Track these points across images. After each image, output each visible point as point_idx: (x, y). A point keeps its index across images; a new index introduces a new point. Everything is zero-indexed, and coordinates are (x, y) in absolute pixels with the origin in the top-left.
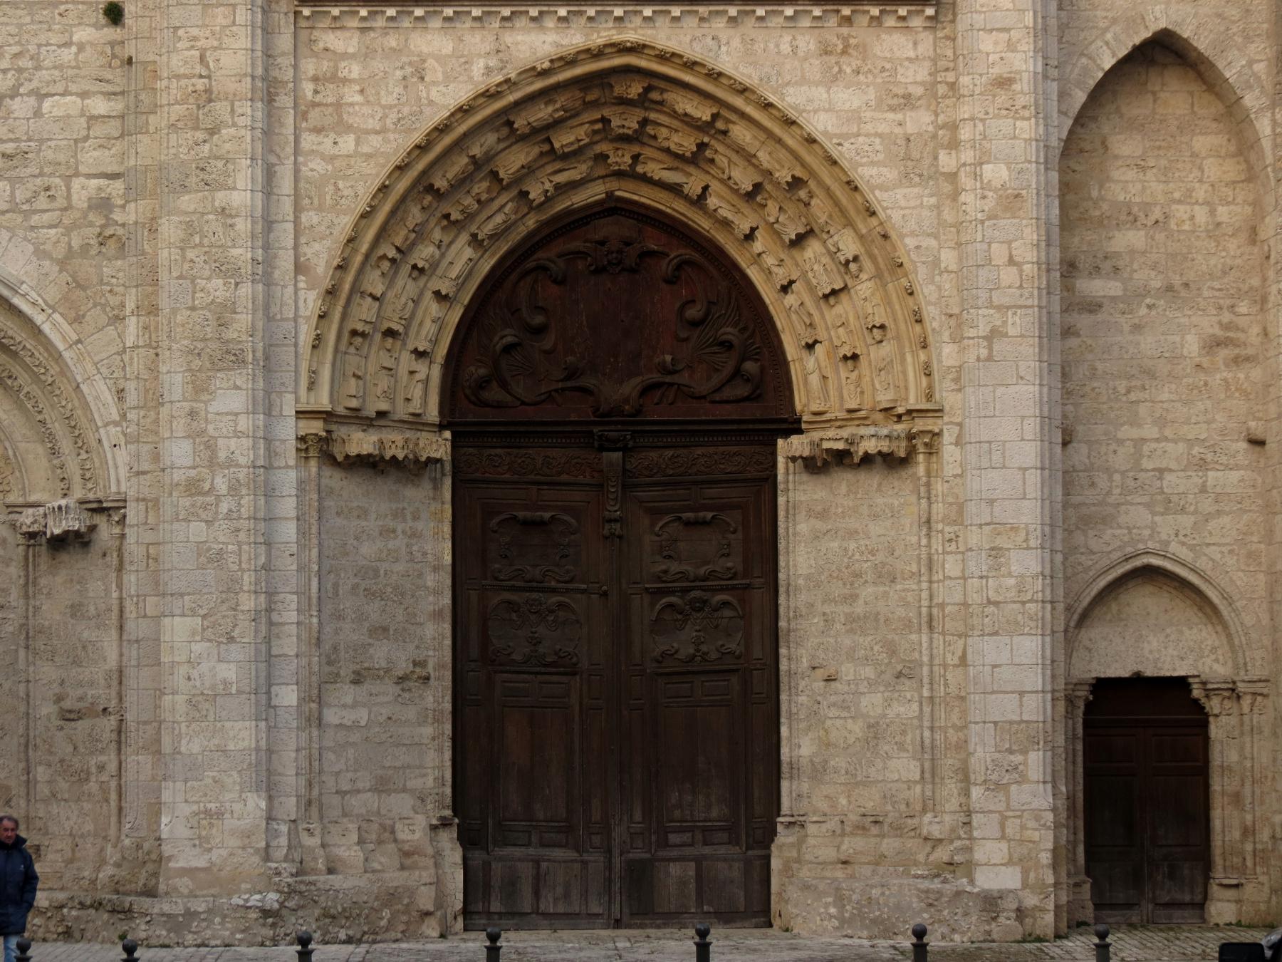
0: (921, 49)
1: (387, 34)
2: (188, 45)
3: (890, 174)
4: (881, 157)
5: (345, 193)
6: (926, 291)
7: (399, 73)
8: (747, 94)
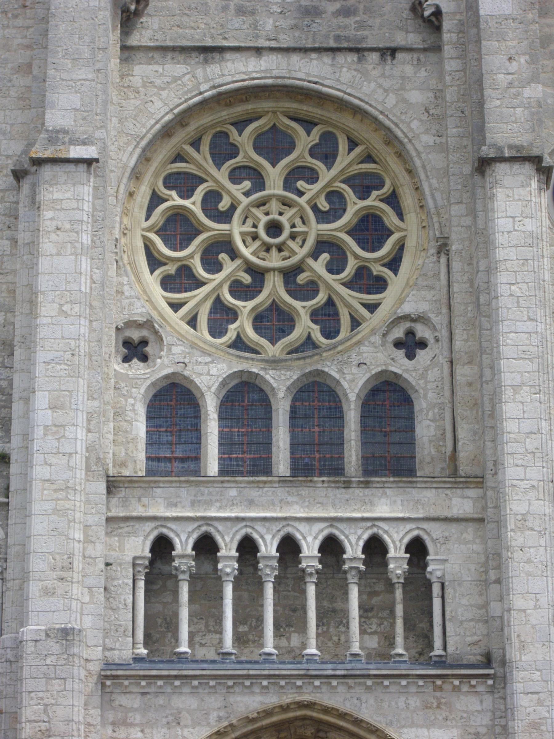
0: (485, 704)
1: (157, 696)
2: (36, 702)
7: (165, 721)
8: (378, 733)
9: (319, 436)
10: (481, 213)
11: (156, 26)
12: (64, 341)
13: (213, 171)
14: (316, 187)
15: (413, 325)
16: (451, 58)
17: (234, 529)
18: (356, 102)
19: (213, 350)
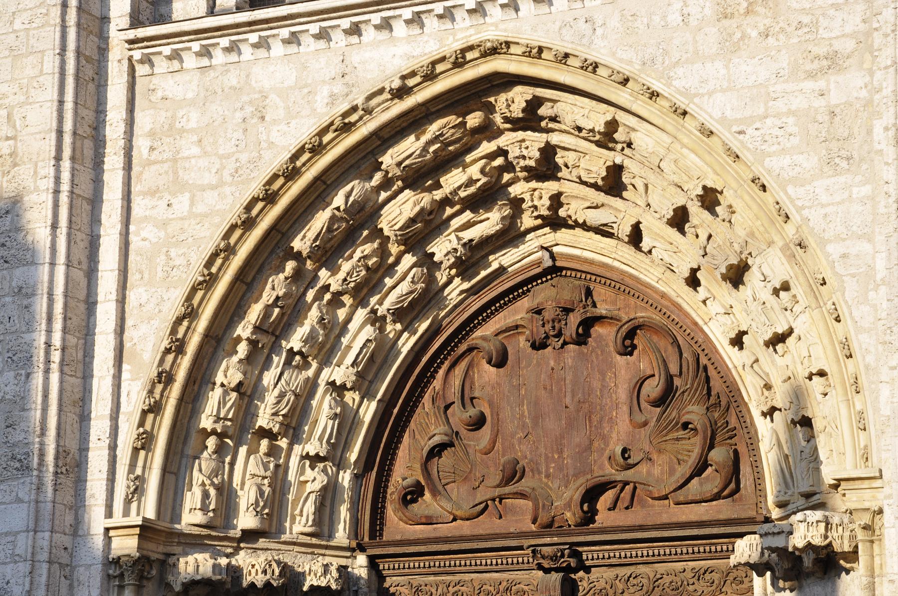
1: (228, 71)
3: (809, 162)
4: (795, 141)
5: (177, 263)
6: (855, 314)
7: (239, 115)
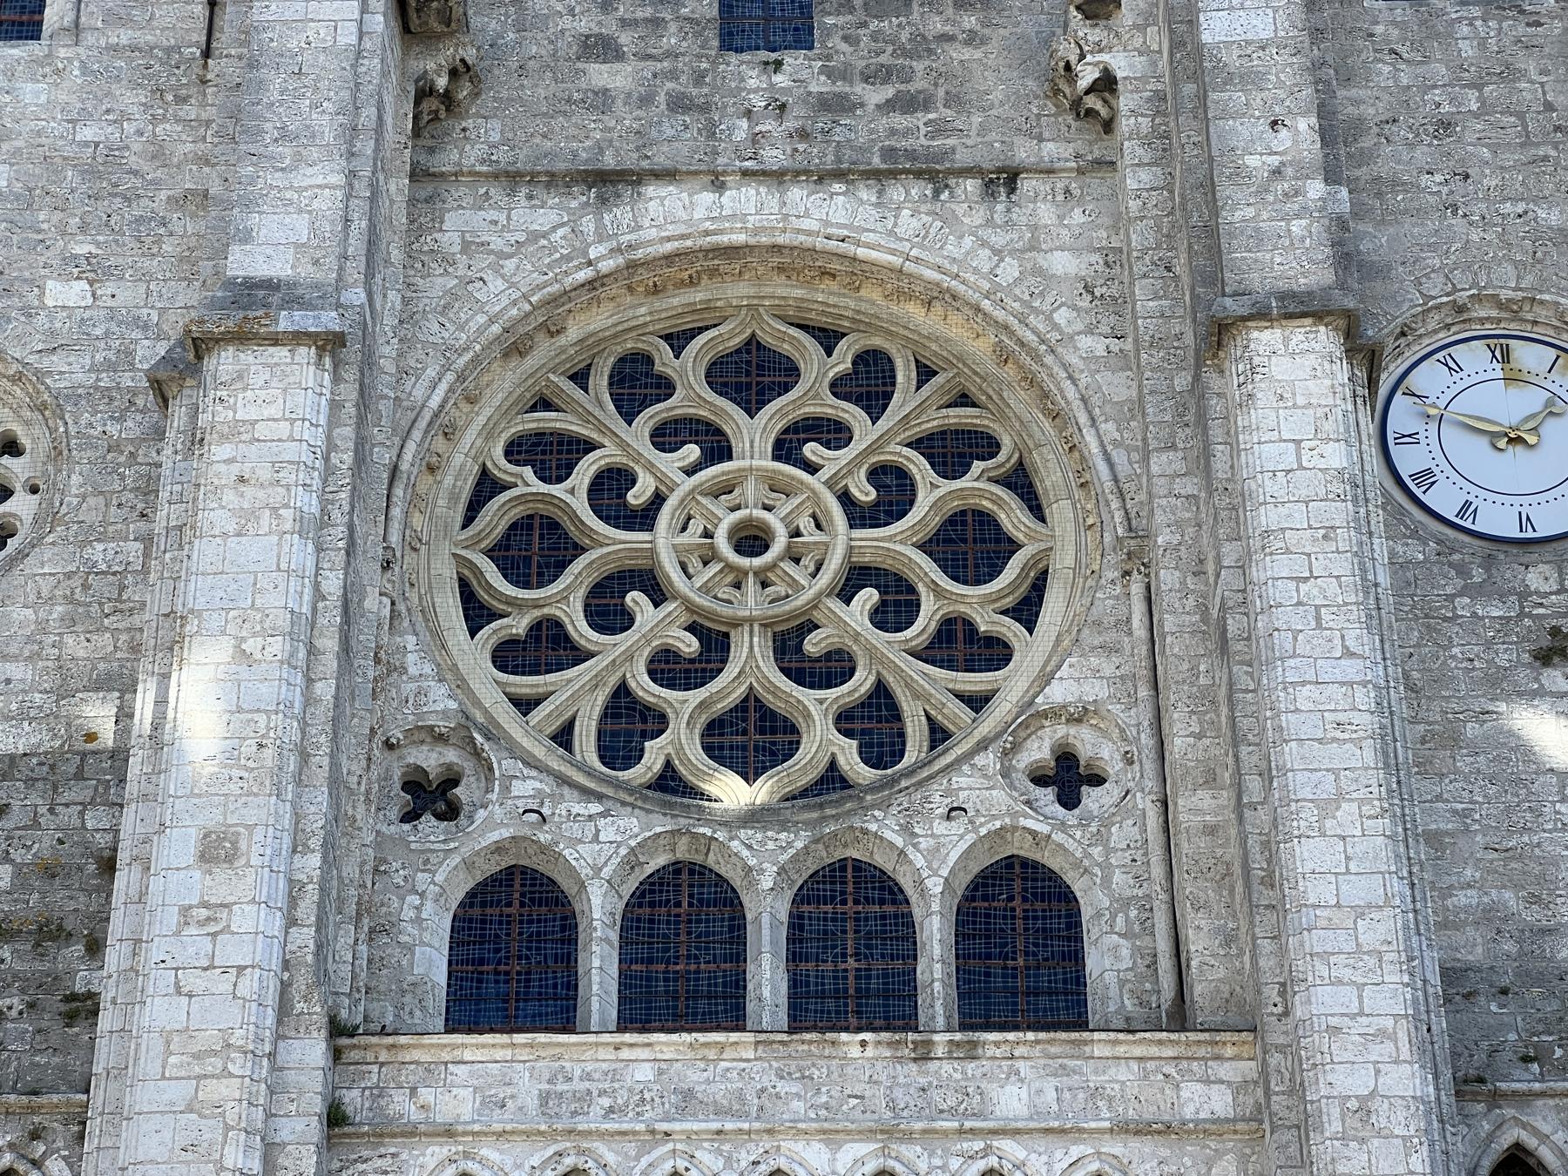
9: (857, 978)
10: (1220, 447)
11: (495, 137)
12: (241, 716)
13: (618, 425)
14: (846, 454)
15: (1072, 731)
16: (1138, 165)
17: (644, 1161)
18: (930, 274)
19: (610, 792)
